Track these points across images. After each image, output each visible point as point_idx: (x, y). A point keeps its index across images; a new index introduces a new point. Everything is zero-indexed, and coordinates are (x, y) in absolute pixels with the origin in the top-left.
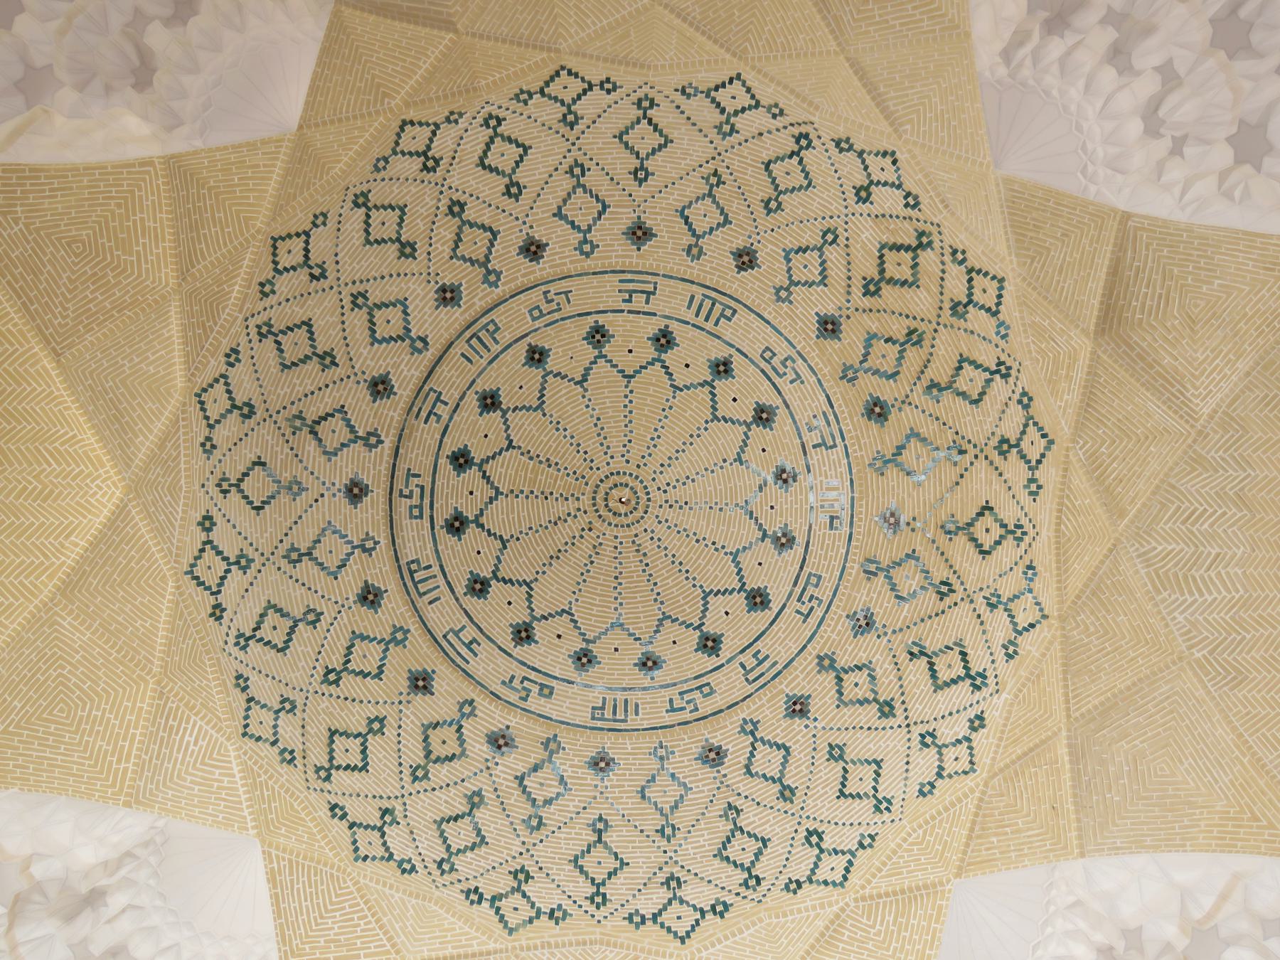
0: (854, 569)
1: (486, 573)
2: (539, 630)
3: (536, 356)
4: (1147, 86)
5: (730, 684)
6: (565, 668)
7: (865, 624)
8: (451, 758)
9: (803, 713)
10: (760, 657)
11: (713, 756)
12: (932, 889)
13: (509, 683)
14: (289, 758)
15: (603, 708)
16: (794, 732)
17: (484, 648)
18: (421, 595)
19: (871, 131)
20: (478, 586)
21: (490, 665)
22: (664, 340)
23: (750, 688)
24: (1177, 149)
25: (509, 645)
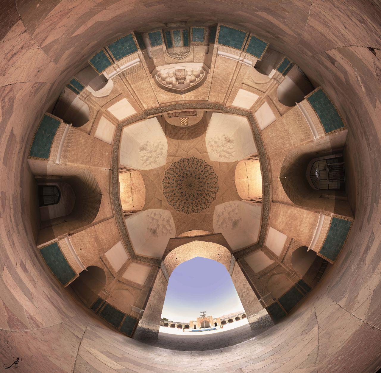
3: (198, 194)
4: (162, 217)
7: (173, 180)
11: (182, 170)
12: (166, 164)
14: (210, 166)
19: (178, 212)
21: (198, 173)
22: (189, 196)
24: (159, 213)
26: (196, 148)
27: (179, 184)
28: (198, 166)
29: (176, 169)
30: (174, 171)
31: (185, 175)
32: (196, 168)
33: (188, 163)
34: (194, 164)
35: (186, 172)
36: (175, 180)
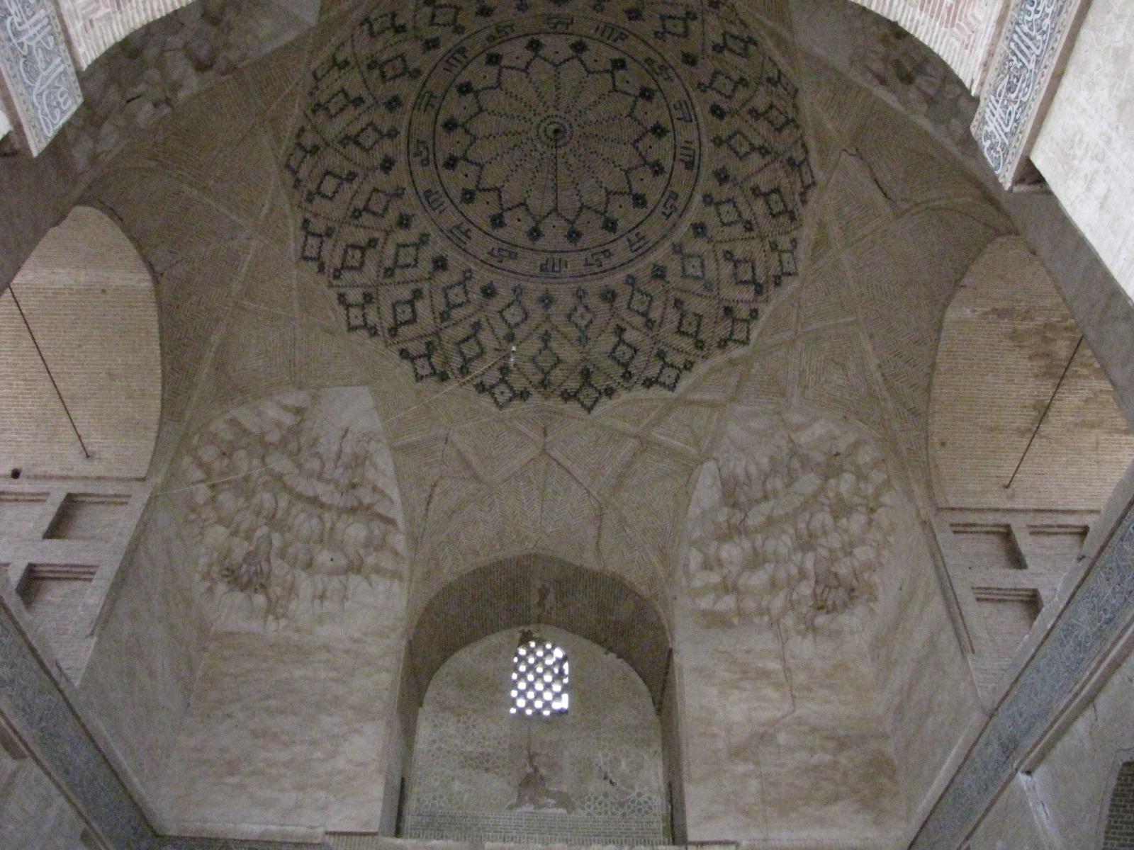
0: (698, 198)
1: (471, 187)
2: (507, 217)
3: (494, 59)
5: (621, 251)
6: (523, 240)
8: (460, 305)
9: (662, 277)
10: (640, 236)
11: (609, 296)
13: (491, 253)
15: (546, 264)
16: (655, 288)
17: (474, 233)
18: (434, 209)
20: (468, 196)
21: (480, 244)
23: (632, 255)
25: (489, 230)
26: (476, 477)
27: (657, 169)
28: (470, 309)
29: (655, 315)
30: (678, 303)
31: (593, 235)
32: (489, 292)
33: (553, 344)
34: (502, 331)
35: (576, 262)
36: (684, 228)
